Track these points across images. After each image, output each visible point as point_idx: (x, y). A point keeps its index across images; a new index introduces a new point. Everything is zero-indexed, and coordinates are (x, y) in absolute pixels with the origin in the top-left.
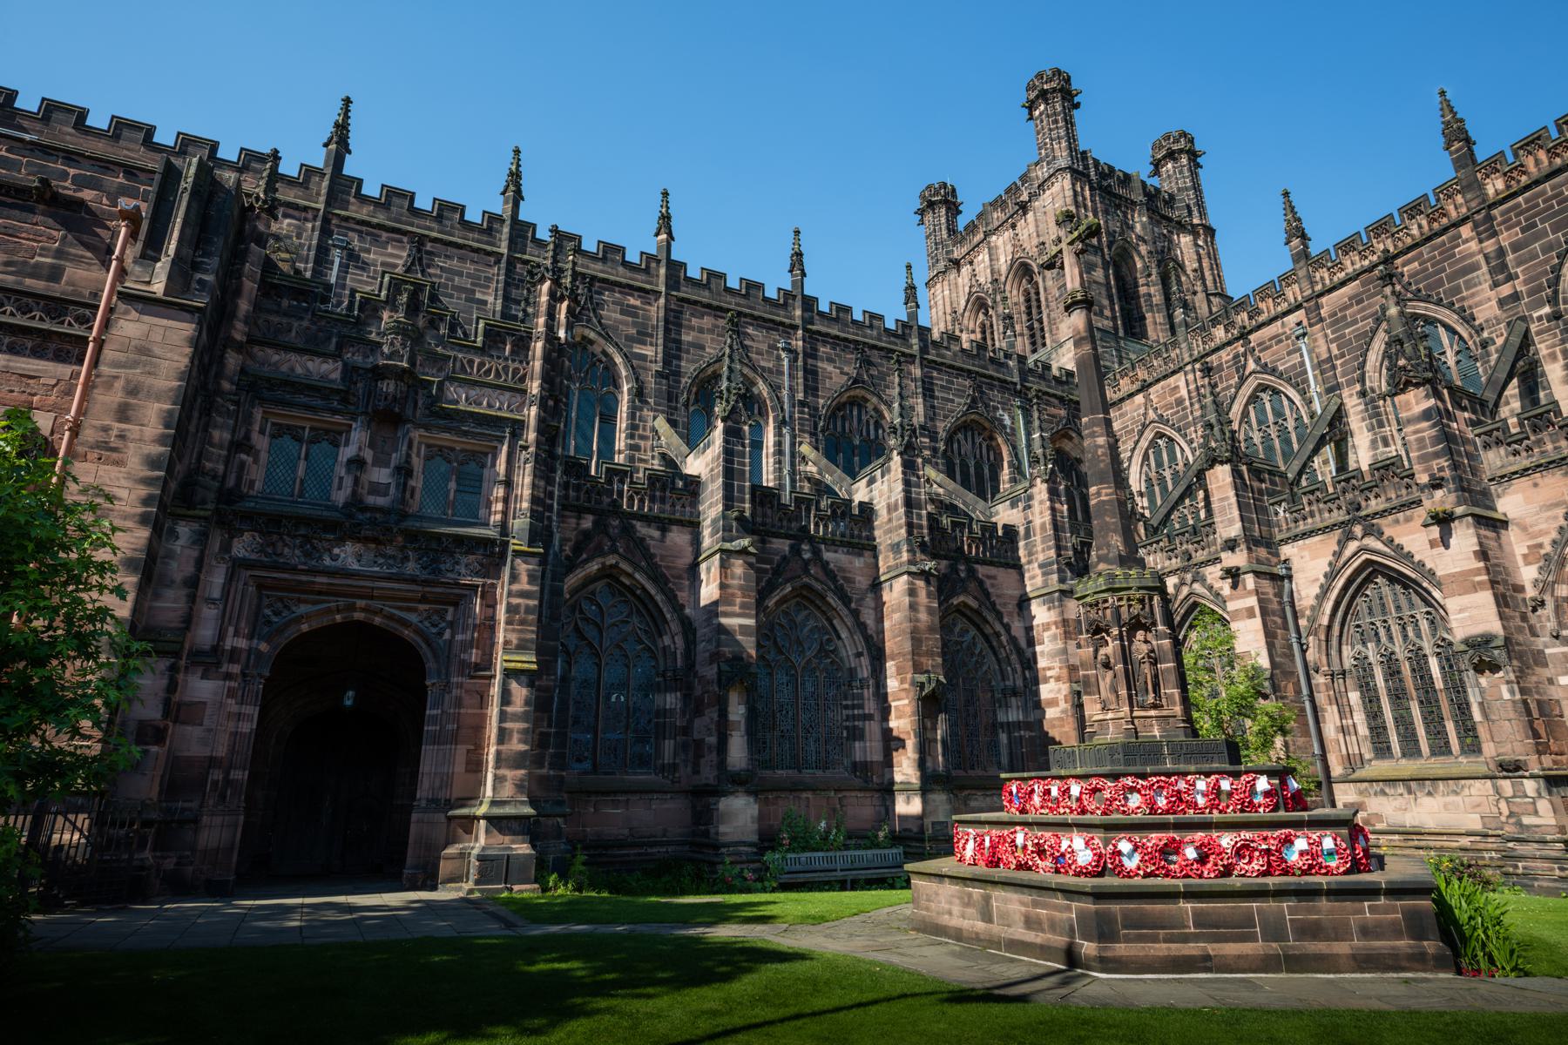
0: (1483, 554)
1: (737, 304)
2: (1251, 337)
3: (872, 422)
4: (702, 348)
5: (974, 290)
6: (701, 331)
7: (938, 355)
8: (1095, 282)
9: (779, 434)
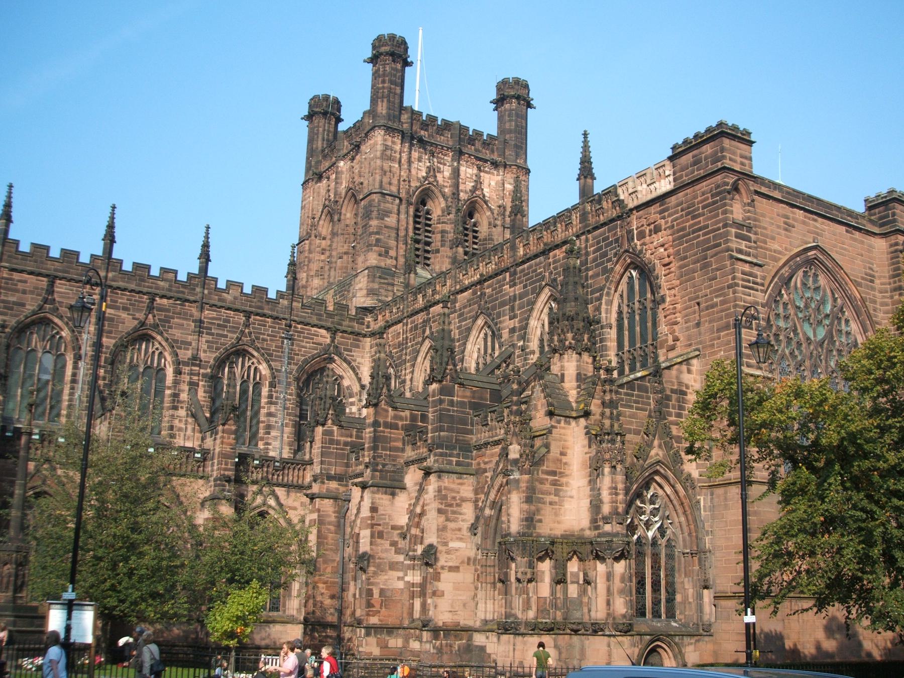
0: (374, 509)
1: (56, 270)
2: (432, 310)
3: (157, 353)
4: (23, 305)
5: (327, 203)
6: (24, 292)
7: (219, 300)
8: (386, 227)
9: (76, 367)
